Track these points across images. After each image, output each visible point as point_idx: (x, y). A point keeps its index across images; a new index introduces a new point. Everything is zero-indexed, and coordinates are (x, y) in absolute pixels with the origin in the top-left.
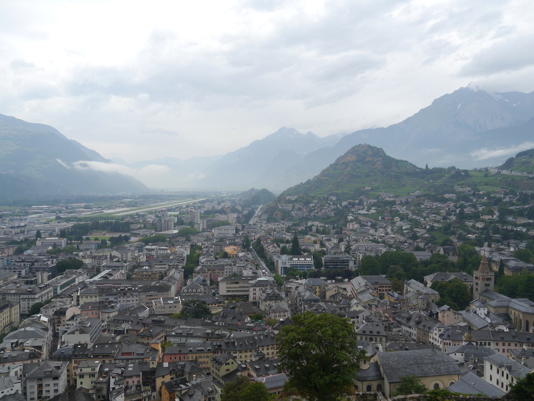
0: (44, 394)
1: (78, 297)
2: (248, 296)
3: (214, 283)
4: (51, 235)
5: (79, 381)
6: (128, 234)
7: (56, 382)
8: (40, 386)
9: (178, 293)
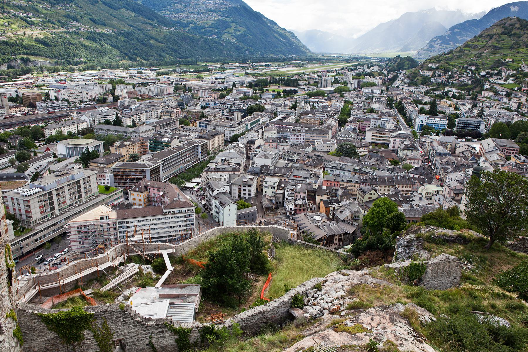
0: (242, 195)
1: (263, 132)
2: (388, 145)
3: (362, 131)
4: (242, 86)
5: (264, 190)
6: (296, 89)
7: (250, 188)
8: (240, 190)
9: (334, 137)
